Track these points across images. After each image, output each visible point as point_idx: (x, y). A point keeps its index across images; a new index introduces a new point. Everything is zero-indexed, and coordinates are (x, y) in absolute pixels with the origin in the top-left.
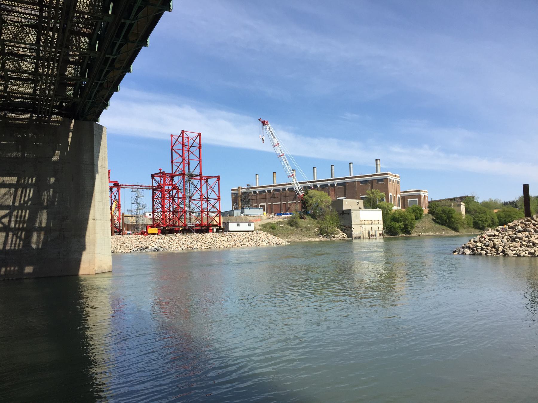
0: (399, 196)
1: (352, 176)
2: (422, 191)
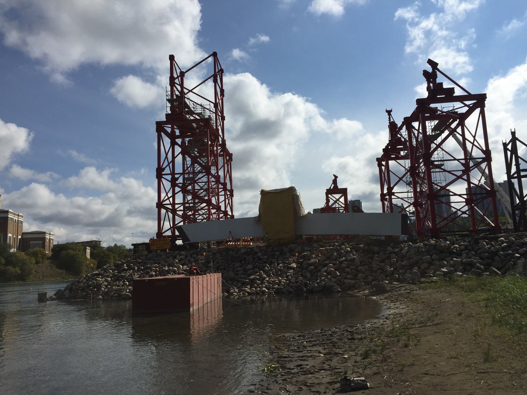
2: (47, 233)
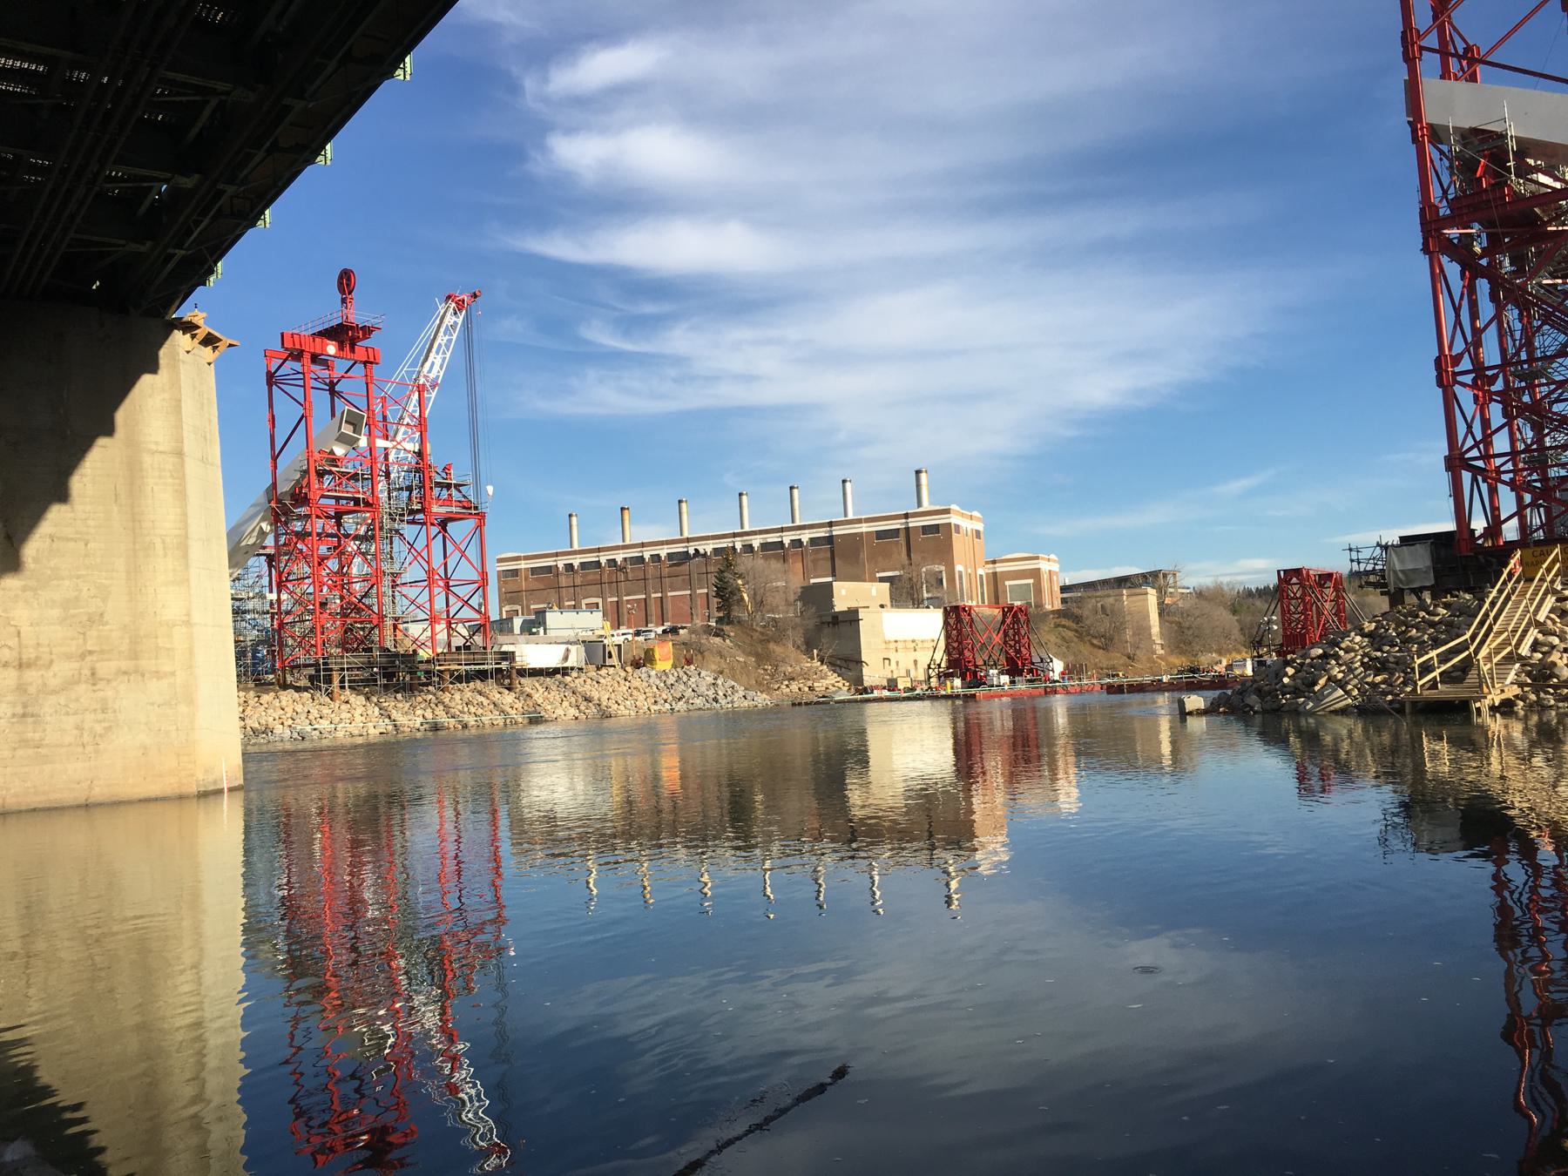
0: (981, 571)
1: (851, 516)
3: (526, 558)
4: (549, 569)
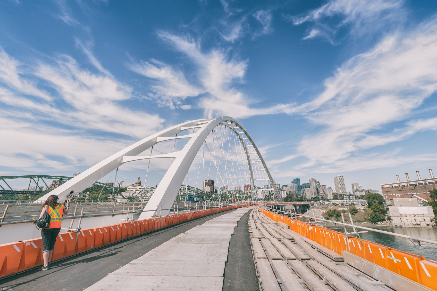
3: (385, 185)
4: (389, 187)
